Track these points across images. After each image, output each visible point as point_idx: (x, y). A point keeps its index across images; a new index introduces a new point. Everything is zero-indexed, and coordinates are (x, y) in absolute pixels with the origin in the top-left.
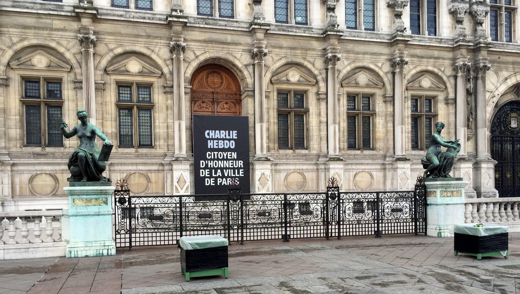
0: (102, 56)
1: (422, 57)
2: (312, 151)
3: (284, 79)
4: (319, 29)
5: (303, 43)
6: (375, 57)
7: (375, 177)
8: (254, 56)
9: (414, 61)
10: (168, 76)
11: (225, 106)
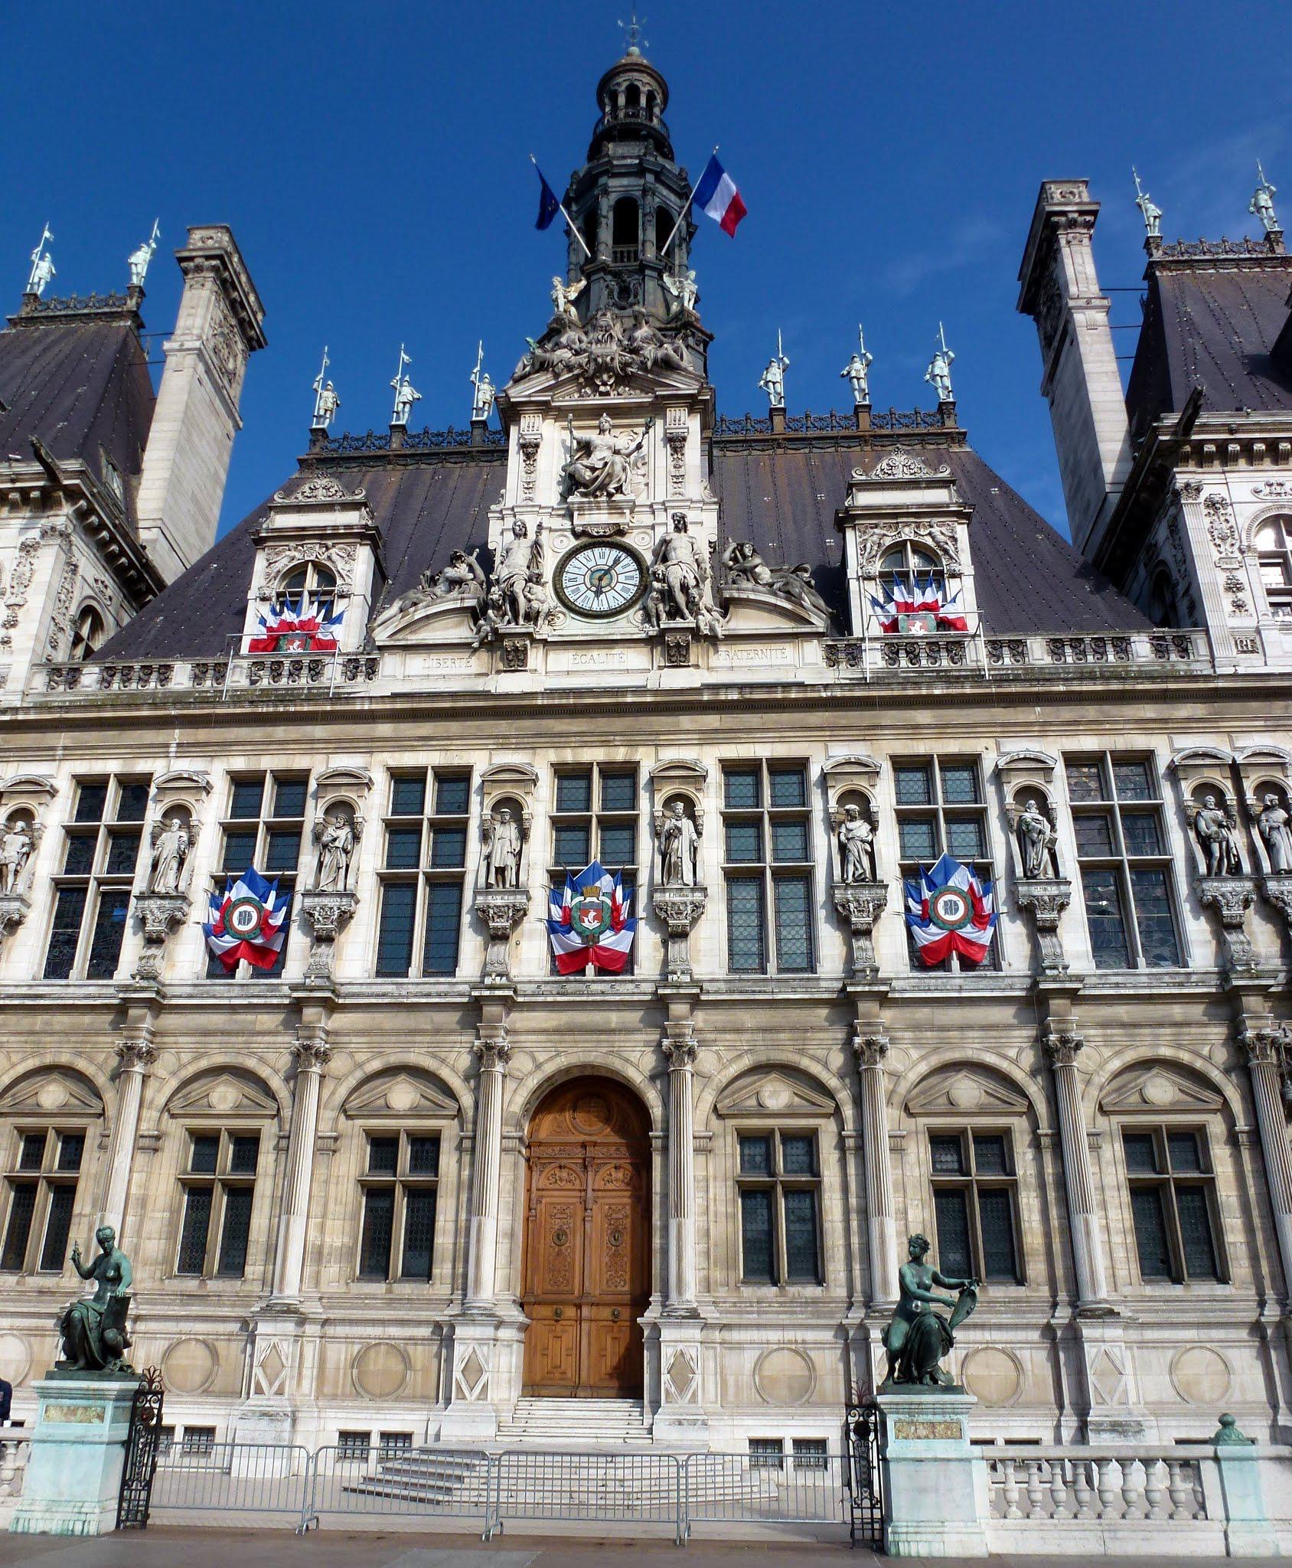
0: (339, 1079)
2: (832, 1289)
4: (836, 979)
5: (796, 1015)
6: (994, 1033)
7: (1028, 1366)
9: (1112, 1035)
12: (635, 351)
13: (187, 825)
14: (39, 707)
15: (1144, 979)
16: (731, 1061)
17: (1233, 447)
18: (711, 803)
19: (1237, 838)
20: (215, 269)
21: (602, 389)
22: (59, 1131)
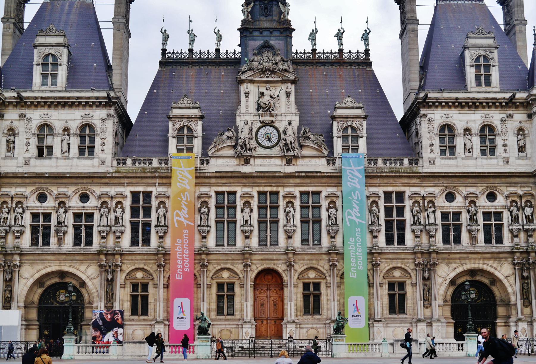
1: (393, 259)
3: (306, 276)
5: (317, 257)
8: (288, 266)
11: (274, 291)
12: (276, 64)
13: (164, 207)
15: (396, 249)
16: (302, 267)
17: (437, 104)
18: (297, 203)
19: (421, 215)
21: (267, 75)
22: (141, 283)
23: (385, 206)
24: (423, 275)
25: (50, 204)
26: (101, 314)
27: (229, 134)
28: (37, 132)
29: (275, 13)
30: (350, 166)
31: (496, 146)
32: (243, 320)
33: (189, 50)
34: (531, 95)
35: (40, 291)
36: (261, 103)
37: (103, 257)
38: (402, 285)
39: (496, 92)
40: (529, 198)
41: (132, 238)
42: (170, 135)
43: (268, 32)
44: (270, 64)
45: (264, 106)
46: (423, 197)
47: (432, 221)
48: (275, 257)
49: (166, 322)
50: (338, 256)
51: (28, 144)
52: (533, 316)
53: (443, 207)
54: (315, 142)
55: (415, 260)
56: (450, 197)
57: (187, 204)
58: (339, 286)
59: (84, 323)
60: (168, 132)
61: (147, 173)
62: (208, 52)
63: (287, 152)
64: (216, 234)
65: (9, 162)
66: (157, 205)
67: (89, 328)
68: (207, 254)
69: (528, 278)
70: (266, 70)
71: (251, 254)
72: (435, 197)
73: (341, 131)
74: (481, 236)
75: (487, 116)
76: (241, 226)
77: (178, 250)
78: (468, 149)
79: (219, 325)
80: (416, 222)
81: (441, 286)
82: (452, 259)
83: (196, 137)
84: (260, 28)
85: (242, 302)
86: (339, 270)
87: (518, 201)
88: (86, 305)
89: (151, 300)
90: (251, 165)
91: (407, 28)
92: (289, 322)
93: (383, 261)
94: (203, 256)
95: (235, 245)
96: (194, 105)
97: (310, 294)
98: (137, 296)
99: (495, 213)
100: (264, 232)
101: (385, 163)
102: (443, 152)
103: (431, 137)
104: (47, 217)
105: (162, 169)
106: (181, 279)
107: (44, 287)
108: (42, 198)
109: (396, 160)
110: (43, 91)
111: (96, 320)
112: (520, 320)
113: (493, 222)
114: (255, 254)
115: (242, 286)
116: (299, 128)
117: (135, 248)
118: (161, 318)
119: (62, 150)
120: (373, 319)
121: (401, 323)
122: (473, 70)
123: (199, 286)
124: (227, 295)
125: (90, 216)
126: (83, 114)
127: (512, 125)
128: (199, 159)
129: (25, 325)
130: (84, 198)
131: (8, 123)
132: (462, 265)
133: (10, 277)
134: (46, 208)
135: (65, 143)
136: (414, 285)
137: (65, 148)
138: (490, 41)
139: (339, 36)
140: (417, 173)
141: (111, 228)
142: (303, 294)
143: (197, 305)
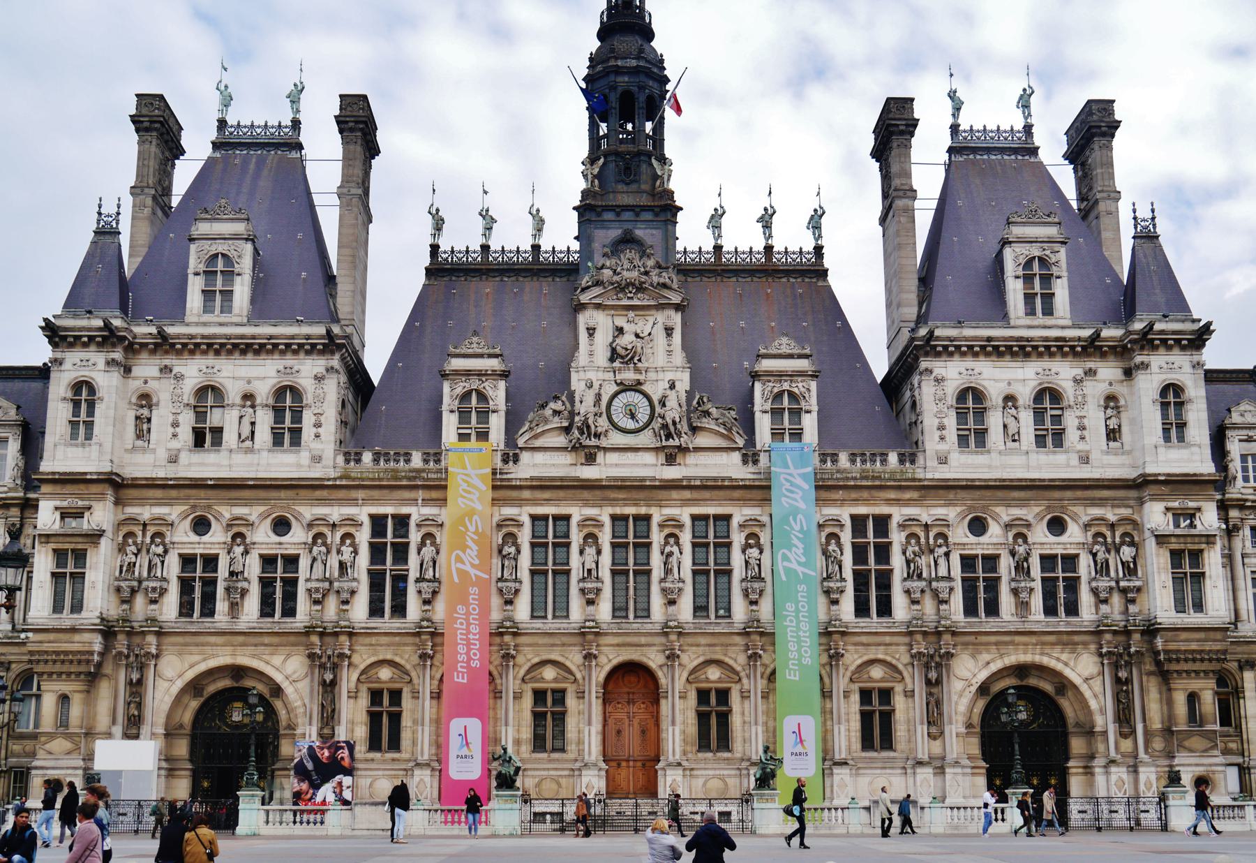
0: (520, 667)
1: (868, 645)
3: (704, 676)
8: (668, 658)
10: (581, 681)
12: (646, 273)
13: (434, 544)
14: (346, 477)
17: (951, 349)
18: (686, 538)
19: (923, 561)
20: (361, 130)
21: (629, 295)
23: (853, 543)
24: (926, 676)
25: (216, 538)
26: (311, 748)
27: (558, 406)
28: (192, 402)
29: (644, 177)
30: (787, 467)
31: (1064, 429)
32: (583, 761)
33: (482, 246)
34: (1131, 333)
35: (194, 704)
36: (618, 348)
37: (315, 639)
38: (886, 695)
39: (1063, 327)
40: (1129, 528)
41: (371, 602)
42: (445, 407)
43: (631, 213)
44: (635, 274)
45: (623, 352)
46: (927, 527)
47: (943, 571)
48: (643, 640)
49: (435, 764)
50: (764, 639)
51: (175, 425)
52: (1137, 755)
53: (964, 544)
54: (720, 421)
55: (911, 646)
56: (978, 526)
57: (476, 538)
58: (765, 696)
59: (278, 766)
60: (441, 402)
61: (400, 479)
62: (518, 251)
63: (667, 439)
64: (532, 596)
65: (139, 458)
66: (419, 540)
67: (288, 776)
68: (515, 634)
69: (1128, 681)
70: (628, 285)
71: (597, 634)
72: (948, 526)
73: (770, 401)
74: (1037, 602)
75: (1048, 372)
76: (579, 581)
77: (460, 626)
78: (1010, 434)
79: (537, 769)
80: (913, 573)
81: (961, 696)
82: (981, 644)
83: (494, 412)
84: (616, 206)
85: (581, 725)
86: (765, 666)
87: (1108, 534)
88: (282, 732)
89: (406, 721)
90: (599, 464)
91: (894, 206)
92: (669, 765)
93: (849, 648)
94: (507, 638)
95: (567, 617)
96: (491, 351)
97: (711, 712)
98: (381, 713)
99: (1064, 557)
100: (623, 593)
101: (853, 462)
102: (963, 441)
103: (941, 412)
104: (211, 562)
105: (430, 471)
106: (465, 681)
107: (202, 696)
108: (201, 526)
109: (874, 455)
110: (205, 324)
111: (302, 760)
112: (1113, 762)
113: (1061, 575)
114: (606, 634)
115: (581, 695)
116: (690, 395)
117: (376, 623)
118: (426, 757)
119: (240, 435)
120: (831, 760)
121: (885, 768)
122: (1019, 284)
123: (498, 695)
124: (552, 712)
125: (292, 561)
126: (281, 368)
127: (1096, 390)
128: (499, 454)
129: (166, 769)
130: (281, 526)
131: (139, 383)
132: (1001, 656)
133: (138, 676)
134: (209, 546)
135: (246, 421)
136: (909, 694)
137: (246, 431)
138: (1052, 231)
139: (766, 221)
140: (914, 480)
141: (331, 583)
142: (697, 711)
143: (495, 732)
